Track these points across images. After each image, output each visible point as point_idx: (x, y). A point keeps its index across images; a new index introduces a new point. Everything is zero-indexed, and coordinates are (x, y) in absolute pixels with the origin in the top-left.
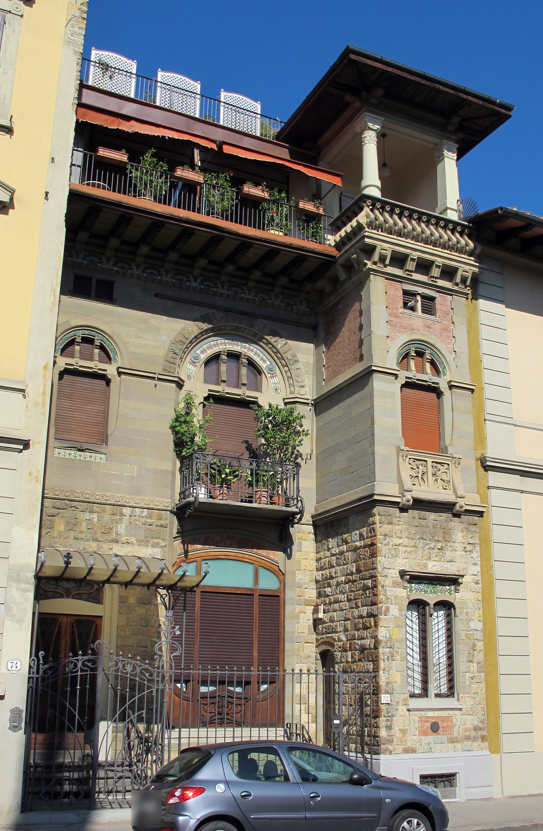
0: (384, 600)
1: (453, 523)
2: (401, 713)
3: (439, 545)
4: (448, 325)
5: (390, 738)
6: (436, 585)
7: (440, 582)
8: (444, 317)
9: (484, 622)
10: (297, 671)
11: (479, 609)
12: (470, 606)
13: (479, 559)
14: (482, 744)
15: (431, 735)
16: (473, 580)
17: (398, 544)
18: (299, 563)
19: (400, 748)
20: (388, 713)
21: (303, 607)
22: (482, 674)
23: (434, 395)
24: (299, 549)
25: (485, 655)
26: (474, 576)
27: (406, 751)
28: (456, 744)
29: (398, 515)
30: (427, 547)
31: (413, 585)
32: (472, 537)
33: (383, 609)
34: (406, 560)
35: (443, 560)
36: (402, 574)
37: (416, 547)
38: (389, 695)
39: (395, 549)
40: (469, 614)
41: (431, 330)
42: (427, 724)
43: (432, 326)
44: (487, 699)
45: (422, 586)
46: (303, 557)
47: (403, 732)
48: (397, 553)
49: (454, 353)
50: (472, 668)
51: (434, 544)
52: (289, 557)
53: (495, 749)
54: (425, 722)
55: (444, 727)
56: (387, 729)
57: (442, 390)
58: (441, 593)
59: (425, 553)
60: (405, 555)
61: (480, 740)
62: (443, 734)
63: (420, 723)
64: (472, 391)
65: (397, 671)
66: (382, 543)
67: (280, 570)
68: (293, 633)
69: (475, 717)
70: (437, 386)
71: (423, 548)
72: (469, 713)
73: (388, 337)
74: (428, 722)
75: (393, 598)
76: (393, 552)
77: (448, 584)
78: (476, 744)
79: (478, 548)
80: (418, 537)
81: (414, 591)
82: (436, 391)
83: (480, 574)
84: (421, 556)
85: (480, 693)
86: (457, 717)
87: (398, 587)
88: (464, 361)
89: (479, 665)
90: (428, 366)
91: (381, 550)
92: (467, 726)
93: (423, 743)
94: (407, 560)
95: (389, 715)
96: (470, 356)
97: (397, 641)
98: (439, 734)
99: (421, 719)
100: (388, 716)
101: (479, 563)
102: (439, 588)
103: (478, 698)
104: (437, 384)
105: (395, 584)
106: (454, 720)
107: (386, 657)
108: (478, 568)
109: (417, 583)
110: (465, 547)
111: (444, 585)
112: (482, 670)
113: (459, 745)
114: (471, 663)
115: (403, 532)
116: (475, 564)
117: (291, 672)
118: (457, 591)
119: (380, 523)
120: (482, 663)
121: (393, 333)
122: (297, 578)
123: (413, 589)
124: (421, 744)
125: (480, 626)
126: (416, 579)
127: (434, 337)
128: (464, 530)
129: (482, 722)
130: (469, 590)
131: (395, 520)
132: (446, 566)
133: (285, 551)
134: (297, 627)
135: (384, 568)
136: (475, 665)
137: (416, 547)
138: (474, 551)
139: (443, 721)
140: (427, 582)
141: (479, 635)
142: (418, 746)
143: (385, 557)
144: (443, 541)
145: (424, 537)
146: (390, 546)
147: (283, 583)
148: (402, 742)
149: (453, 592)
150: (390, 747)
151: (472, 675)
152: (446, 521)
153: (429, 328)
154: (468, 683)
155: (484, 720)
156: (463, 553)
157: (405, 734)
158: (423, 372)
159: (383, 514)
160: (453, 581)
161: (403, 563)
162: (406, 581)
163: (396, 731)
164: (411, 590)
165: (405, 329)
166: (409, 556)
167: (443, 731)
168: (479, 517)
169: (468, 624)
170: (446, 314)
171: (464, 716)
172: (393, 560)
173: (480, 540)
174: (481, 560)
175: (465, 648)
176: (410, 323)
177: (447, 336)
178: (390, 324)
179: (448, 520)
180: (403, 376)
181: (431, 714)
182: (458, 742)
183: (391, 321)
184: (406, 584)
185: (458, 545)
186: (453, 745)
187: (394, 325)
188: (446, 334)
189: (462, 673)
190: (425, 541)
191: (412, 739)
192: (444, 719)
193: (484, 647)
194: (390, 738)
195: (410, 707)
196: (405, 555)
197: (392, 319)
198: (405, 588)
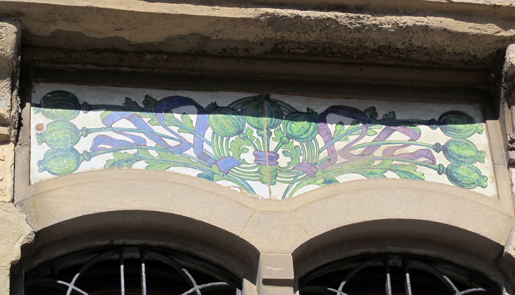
7: (362, 105)
77: (437, 111)
81: (98, 162)
111: (391, 121)
123: (84, 144)
140: (225, 99)
149: (485, 168)
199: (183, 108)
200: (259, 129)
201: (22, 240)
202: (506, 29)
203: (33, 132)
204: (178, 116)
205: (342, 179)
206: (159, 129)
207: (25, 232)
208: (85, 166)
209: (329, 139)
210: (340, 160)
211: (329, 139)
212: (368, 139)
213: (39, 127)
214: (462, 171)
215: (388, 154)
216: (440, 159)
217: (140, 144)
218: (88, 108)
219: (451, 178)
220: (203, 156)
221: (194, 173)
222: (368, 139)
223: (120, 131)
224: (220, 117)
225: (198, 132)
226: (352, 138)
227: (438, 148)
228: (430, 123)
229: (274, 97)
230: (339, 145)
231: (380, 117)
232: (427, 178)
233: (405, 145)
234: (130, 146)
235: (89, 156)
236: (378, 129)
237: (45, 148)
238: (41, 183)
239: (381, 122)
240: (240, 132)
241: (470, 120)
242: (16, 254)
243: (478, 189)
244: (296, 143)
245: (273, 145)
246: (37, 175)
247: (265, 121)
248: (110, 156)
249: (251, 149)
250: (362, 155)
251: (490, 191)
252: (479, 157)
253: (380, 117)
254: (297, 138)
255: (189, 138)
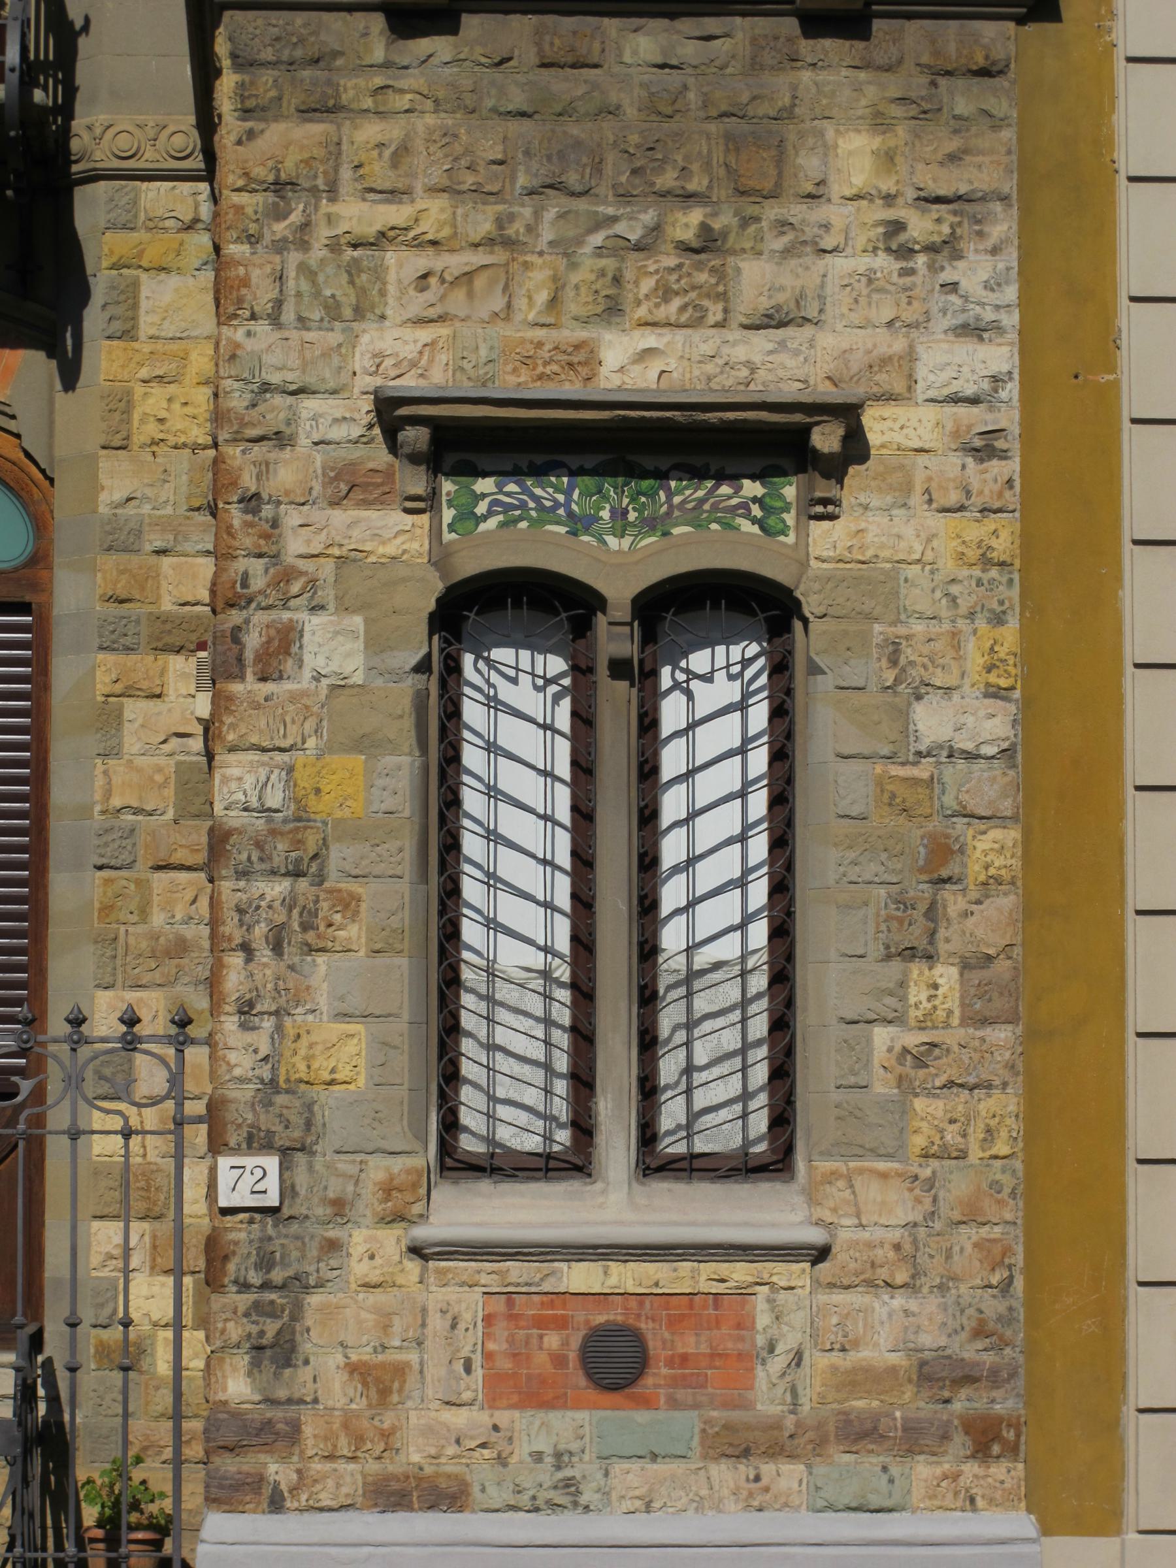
0: (258, 583)
1: (806, 76)
2: (360, 1269)
3: (686, 224)
5: (277, 1414)
6: (662, 476)
7: (697, 461)
9: (1027, 704)
10: (104, 1023)
11: (998, 619)
12: (918, 597)
13: (1011, 293)
14: (971, 1469)
15: (577, 1406)
16: (956, 434)
17: (370, 231)
18: (121, 404)
19: (350, 1476)
20: (266, 1262)
21: (142, 665)
22: (1001, 1035)
24: (117, 326)
25: (1029, 911)
26: (962, 410)
27: (391, 1495)
28: (767, 1469)
29: (378, 54)
30: (597, 239)
31: (484, 485)
32: (953, 158)
33: (253, 641)
34: (425, 335)
35: (715, 312)
36: (390, 413)
37: (509, 243)
38: (272, 1163)
39: (353, 270)
40: (908, 653)
42: (552, 1340)
44: (1031, 1191)
45: (547, 491)
46: (144, 373)
47: (380, 1381)
48: (362, 292)
50: (917, 994)
51: (648, 217)
52: (70, 376)
53: (1081, 1499)
54: (541, 1323)
55: (684, 1359)
56: (255, 1364)
58: (698, 524)
59: (575, 278)
60: (417, 304)
61: (960, 1443)
62: (674, 1404)
63: (501, 1329)
65: (343, 1016)
66: (253, 240)
67: (28, 455)
68: (84, 811)
69: (928, 1306)
71: (565, 248)
72: (883, 1273)
74: (561, 1324)
75: (326, 569)
76: (335, 286)
77: (758, 465)
78: (923, 1470)
79: (1003, 226)
80: (522, 180)
81: (492, 523)
83: (1010, 392)
84: (542, 297)
85: (975, 1154)
86: (787, 1306)
87: (366, 504)
89: (976, 976)
91: (245, 282)
92: (865, 1355)
93: (521, 1452)
94: (443, 331)
95: (277, 1276)
97: (354, 832)
98: (647, 1403)
99: (508, 1306)
100: (266, 1286)
101: (1011, 320)
102: (686, 493)
103: (958, 1186)
105: (349, 486)
106: (763, 1320)
107: (260, 930)
108: (999, 356)
109: (515, 473)
110: (897, 227)
111: (721, 477)
112: (1000, 1004)
113: (788, 1476)
114: (916, 969)
115: (419, 160)
116: (974, 331)
117: (67, 1029)
118: (824, 509)
119: (246, 113)
120: (1002, 967)
122: (104, 497)
123: (481, 508)
124: (502, 1460)
125: (992, 726)
126: (455, 442)
128: (897, 111)
129: (980, 1332)
130: (917, 499)
131: (354, 89)
132: (740, 353)
133: (53, 349)
134: (100, 782)
135: (266, 388)
136: (947, 975)
137: (509, 243)
138: (969, 247)
139: (674, 1323)
140: (590, 461)
141: (987, 787)
142: (479, 1470)
143: (275, 319)
144: (721, 192)
145: (572, 179)
146: (319, 252)
147: (40, 524)
148: (359, 1439)
149: (790, 518)
150: (278, 1471)
151: (913, 1039)
152: (755, 66)
154: (883, 1087)
155: (1007, 1319)
156: (883, 262)
157: (384, 1392)
159: (268, 55)
160: (788, 446)
161: (408, 351)
162: (414, 459)
163: (326, 1375)
164: (467, 517)
166: (457, 302)
167: (675, 1382)
168: (1021, 21)
169: (903, 716)
171: (839, 1297)
172: (334, 337)
173: (1025, 168)
174: (1025, 302)
175: (871, 870)
179: (768, 58)
181: (580, 1277)
182: (778, 1451)
184: (416, 482)
185: (836, 213)
186: (744, 1470)
189: (838, 1031)
190: (582, 205)
191: (435, 1424)
192: (684, 1308)
193: (1027, 858)
194: (277, 1414)
195: (421, 1233)
196: (417, 304)
198: (429, 503)
199: (558, 471)
200: (615, 488)
201: (437, 595)
202: (811, 416)
203: (444, 498)
204: (553, 479)
205: (676, 531)
206: (538, 491)
207: (439, 587)
208: (483, 527)
209: (670, 495)
210: (676, 513)
211: (670, 495)
212: (700, 493)
213: (448, 494)
214: (772, 521)
215: (715, 507)
216: (756, 511)
217: (523, 506)
218: (485, 475)
219: (762, 528)
220: (571, 514)
221: (562, 530)
222: (700, 493)
223: (508, 494)
224: (586, 478)
225: (568, 493)
226: (688, 492)
227: (755, 500)
228: (753, 477)
229: (630, 457)
230: (677, 500)
231: (712, 472)
232: (743, 529)
233: (730, 498)
234: (516, 508)
235: (485, 518)
236: (709, 484)
237: (453, 512)
238: (451, 543)
239: (712, 478)
240: (599, 492)
241: (784, 473)
242: (432, 605)
243: (782, 538)
244: (643, 499)
245: (626, 501)
246: (448, 537)
247: (620, 480)
248: (501, 518)
249: (608, 506)
250: (694, 508)
251: (791, 539)
252: (786, 509)
253: (712, 472)
254: (644, 495)
255: (561, 498)
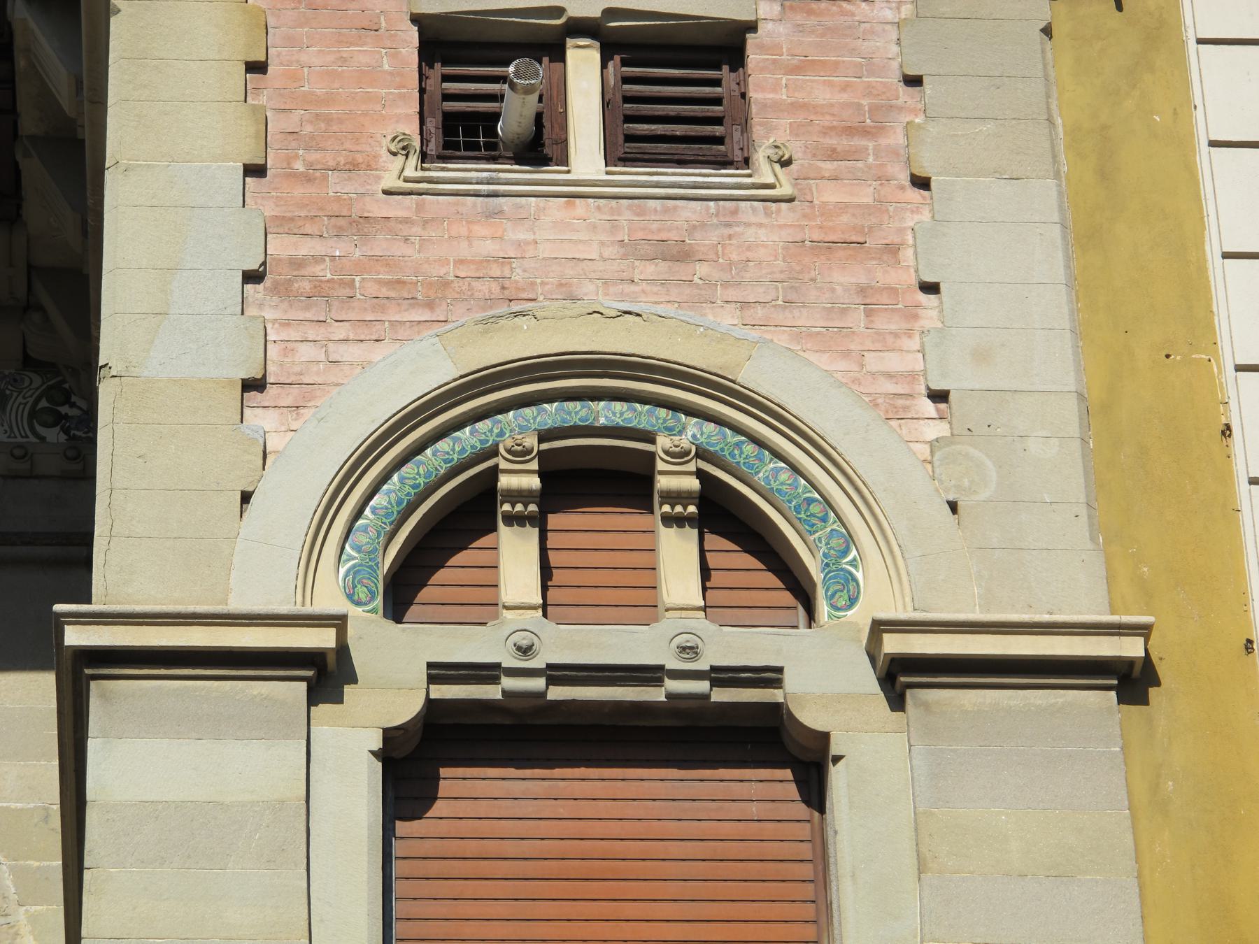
4: (879, 207)
8: (833, 155)
23: (779, 784)
41: (702, 269)
43: (705, 240)
49: (929, 407)
57: (810, 717)
64: (1133, 681)
70: (775, 695)
73: (253, 385)
82: (758, 736)
88: (1051, 452)
90: (677, 555)
96: (1095, 411)
104: (770, 676)
121: (306, 352)
127: (727, 319)
153: (681, 254)
158: (643, 604)
165: (431, 297)
170: (849, 131)
176: (489, 248)
177: (862, 290)
178: (284, 291)
180: (396, 671)
183: (297, 263)
187: (320, 291)
188: (845, 277)
197: (306, 248)
